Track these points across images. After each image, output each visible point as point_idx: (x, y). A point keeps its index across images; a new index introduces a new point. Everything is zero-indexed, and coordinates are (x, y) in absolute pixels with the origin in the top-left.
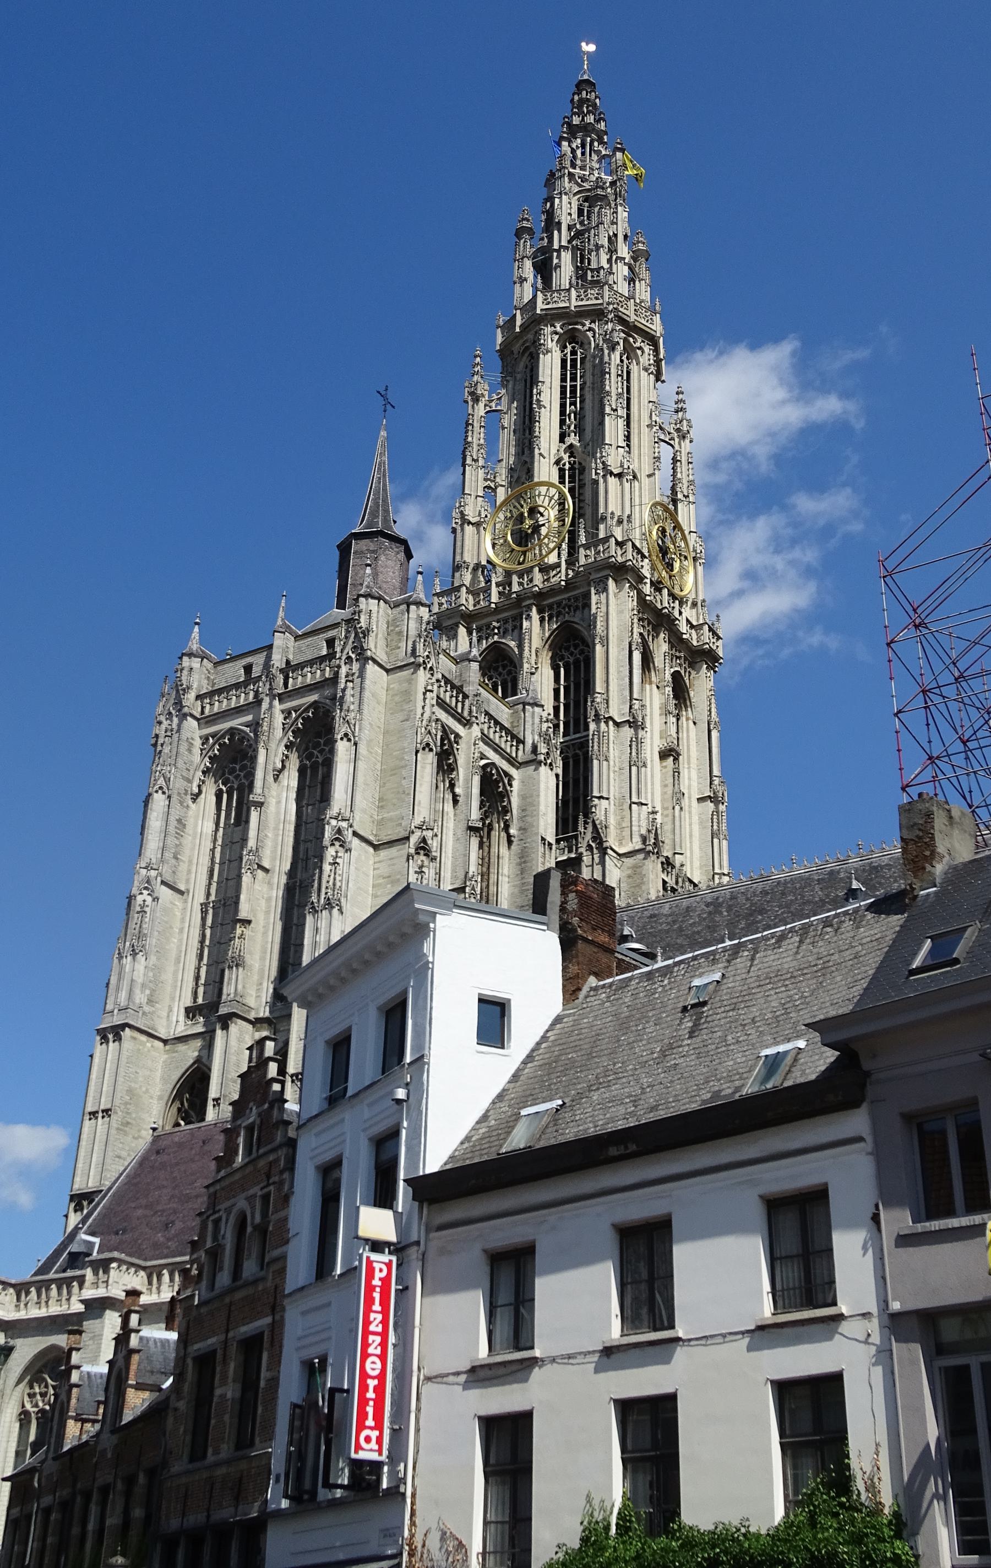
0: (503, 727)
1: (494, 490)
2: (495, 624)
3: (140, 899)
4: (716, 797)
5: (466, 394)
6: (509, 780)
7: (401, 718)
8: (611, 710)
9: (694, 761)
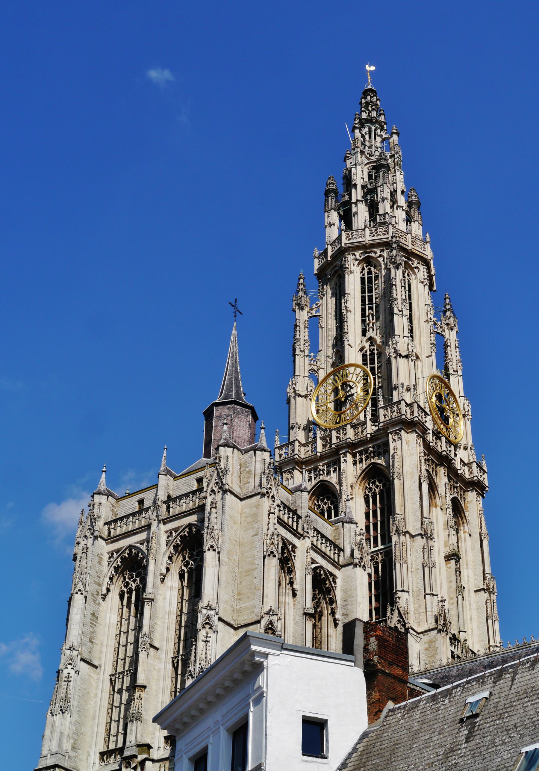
0: (327, 539)
1: (317, 372)
2: (321, 467)
3: (65, 672)
4: (488, 589)
5: (294, 305)
6: (334, 579)
7: (252, 534)
8: (407, 526)
9: (470, 563)
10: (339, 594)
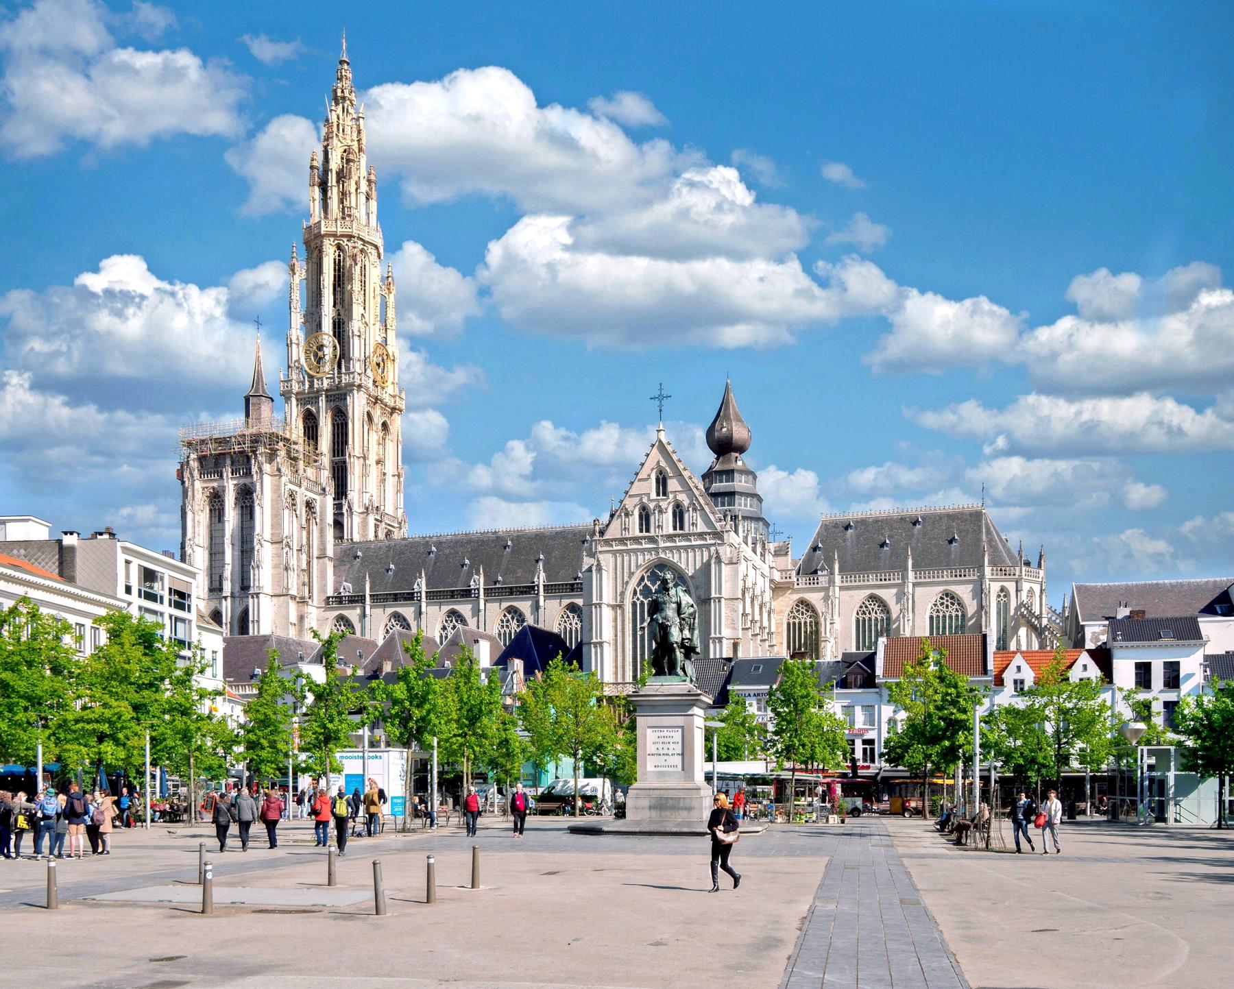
10: (318, 509)
